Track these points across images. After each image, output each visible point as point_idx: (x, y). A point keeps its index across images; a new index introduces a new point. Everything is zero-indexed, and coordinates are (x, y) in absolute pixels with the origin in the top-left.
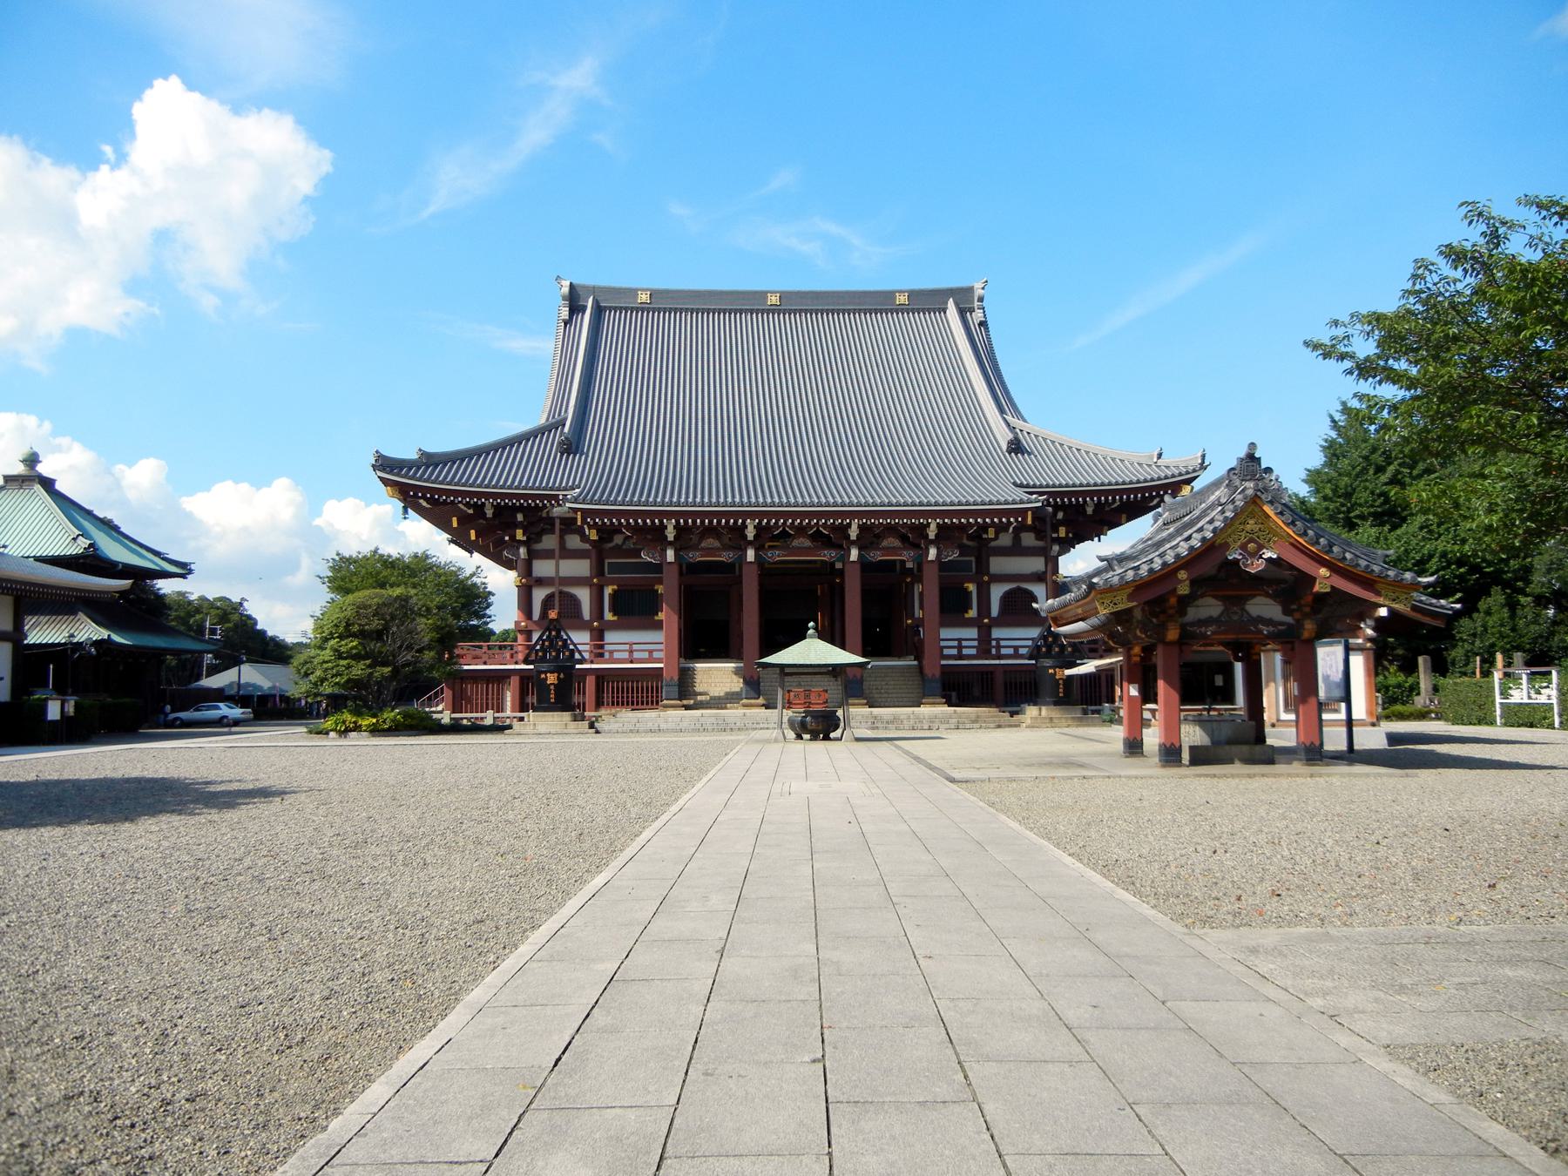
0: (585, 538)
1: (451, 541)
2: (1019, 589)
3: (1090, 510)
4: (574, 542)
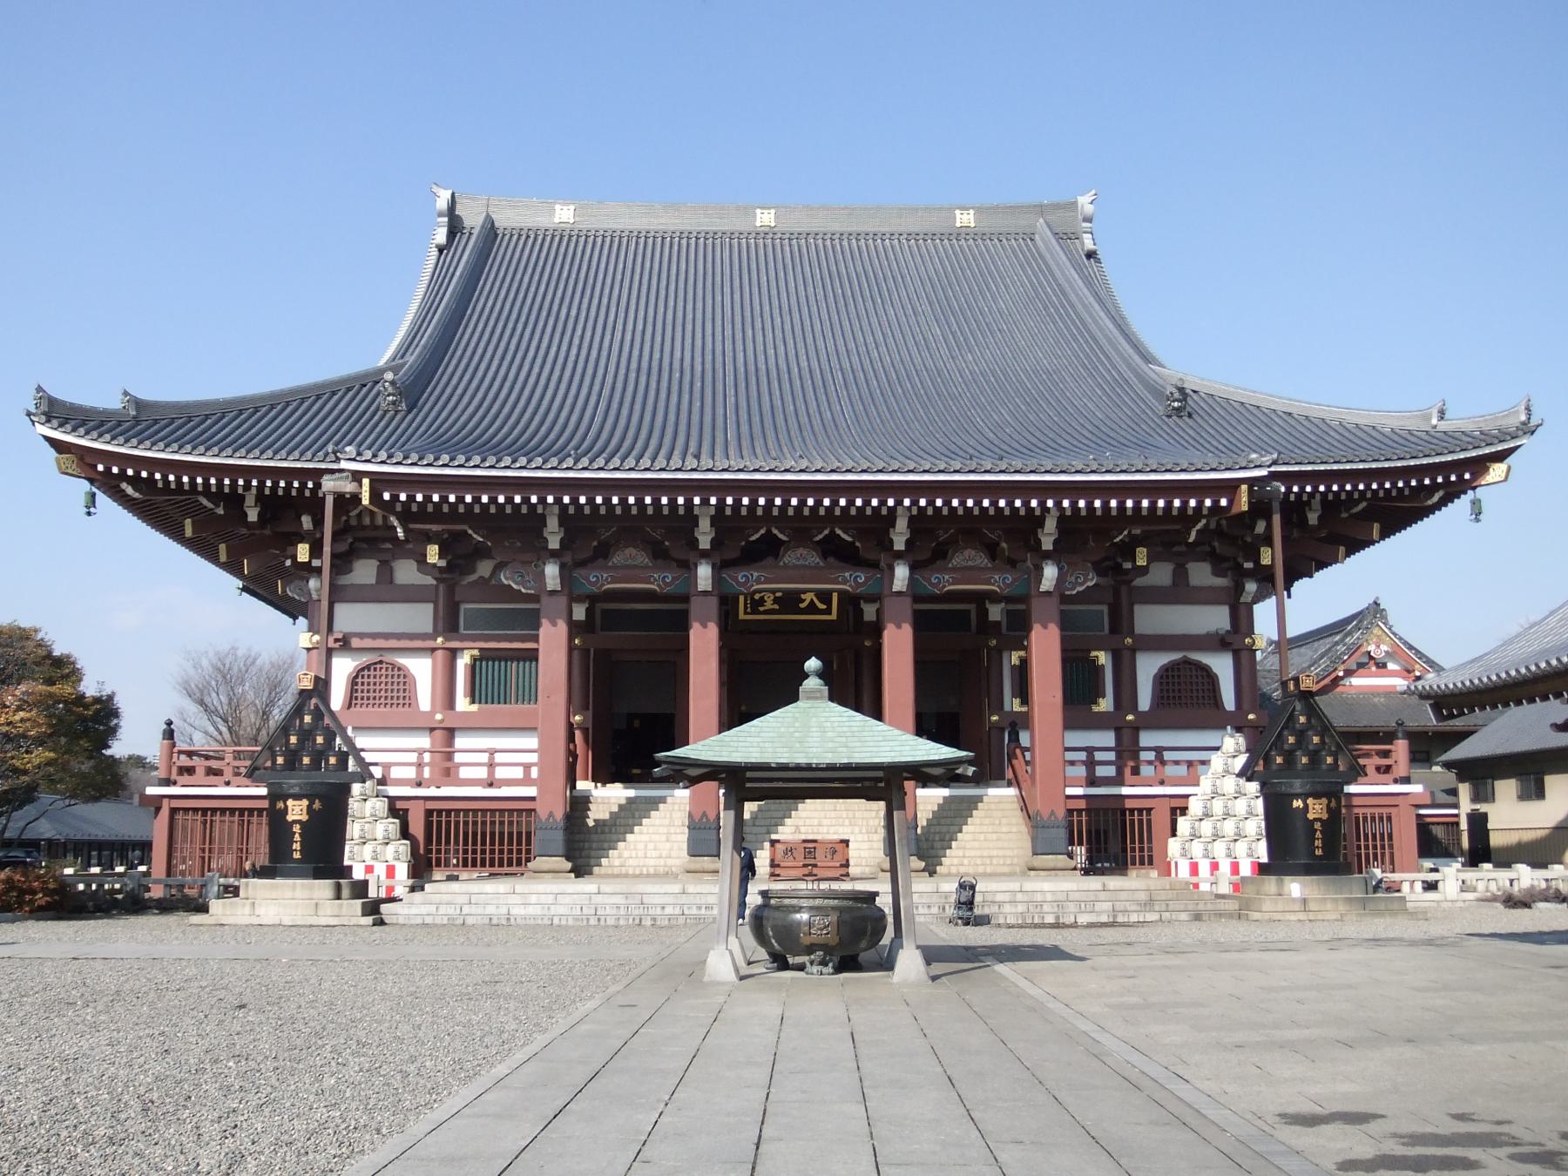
1: (244, 589)
2: (1187, 662)
3: (1313, 518)
4: (406, 572)
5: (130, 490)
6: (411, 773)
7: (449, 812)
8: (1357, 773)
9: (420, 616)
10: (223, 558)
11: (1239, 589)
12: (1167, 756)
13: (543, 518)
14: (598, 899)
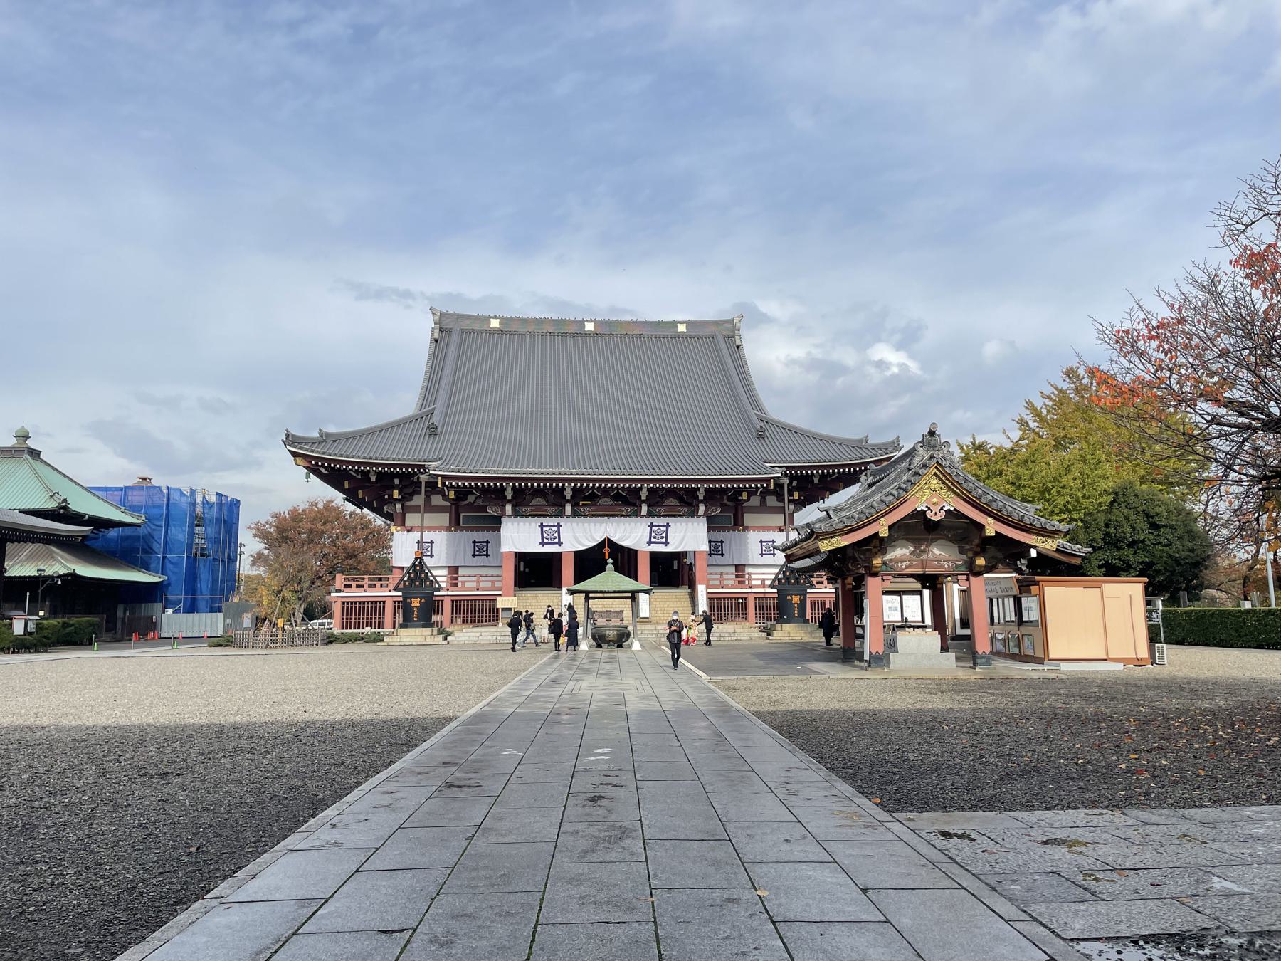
0: (445, 497)
3: (816, 480)
4: (437, 500)
8: (812, 586)
9: (444, 519)
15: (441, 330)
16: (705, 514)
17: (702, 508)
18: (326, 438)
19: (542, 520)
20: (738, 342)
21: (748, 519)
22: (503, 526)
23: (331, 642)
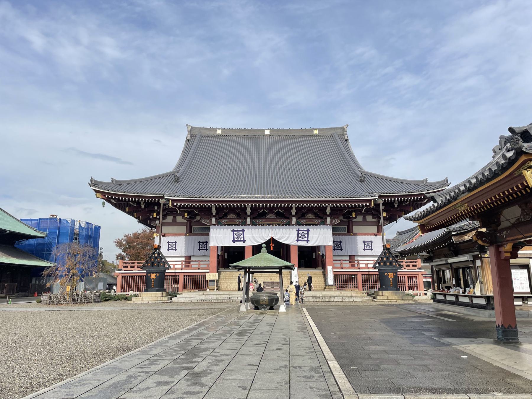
3: (396, 205)
4: (179, 219)
5: (113, 201)
6: (180, 266)
7: (189, 276)
8: (401, 267)
9: (183, 229)
10: (135, 216)
11: (379, 222)
12: (360, 262)
13: (211, 208)
14: (223, 296)
15: (191, 136)
16: (331, 223)
17: (329, 220)
18: (115, 183)
19: (233, 227)
20: (346, 138)
21: (356, 229)
22: (211, 230)
23: (108, 300)
